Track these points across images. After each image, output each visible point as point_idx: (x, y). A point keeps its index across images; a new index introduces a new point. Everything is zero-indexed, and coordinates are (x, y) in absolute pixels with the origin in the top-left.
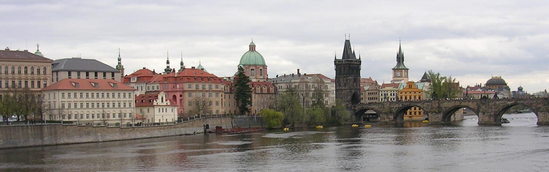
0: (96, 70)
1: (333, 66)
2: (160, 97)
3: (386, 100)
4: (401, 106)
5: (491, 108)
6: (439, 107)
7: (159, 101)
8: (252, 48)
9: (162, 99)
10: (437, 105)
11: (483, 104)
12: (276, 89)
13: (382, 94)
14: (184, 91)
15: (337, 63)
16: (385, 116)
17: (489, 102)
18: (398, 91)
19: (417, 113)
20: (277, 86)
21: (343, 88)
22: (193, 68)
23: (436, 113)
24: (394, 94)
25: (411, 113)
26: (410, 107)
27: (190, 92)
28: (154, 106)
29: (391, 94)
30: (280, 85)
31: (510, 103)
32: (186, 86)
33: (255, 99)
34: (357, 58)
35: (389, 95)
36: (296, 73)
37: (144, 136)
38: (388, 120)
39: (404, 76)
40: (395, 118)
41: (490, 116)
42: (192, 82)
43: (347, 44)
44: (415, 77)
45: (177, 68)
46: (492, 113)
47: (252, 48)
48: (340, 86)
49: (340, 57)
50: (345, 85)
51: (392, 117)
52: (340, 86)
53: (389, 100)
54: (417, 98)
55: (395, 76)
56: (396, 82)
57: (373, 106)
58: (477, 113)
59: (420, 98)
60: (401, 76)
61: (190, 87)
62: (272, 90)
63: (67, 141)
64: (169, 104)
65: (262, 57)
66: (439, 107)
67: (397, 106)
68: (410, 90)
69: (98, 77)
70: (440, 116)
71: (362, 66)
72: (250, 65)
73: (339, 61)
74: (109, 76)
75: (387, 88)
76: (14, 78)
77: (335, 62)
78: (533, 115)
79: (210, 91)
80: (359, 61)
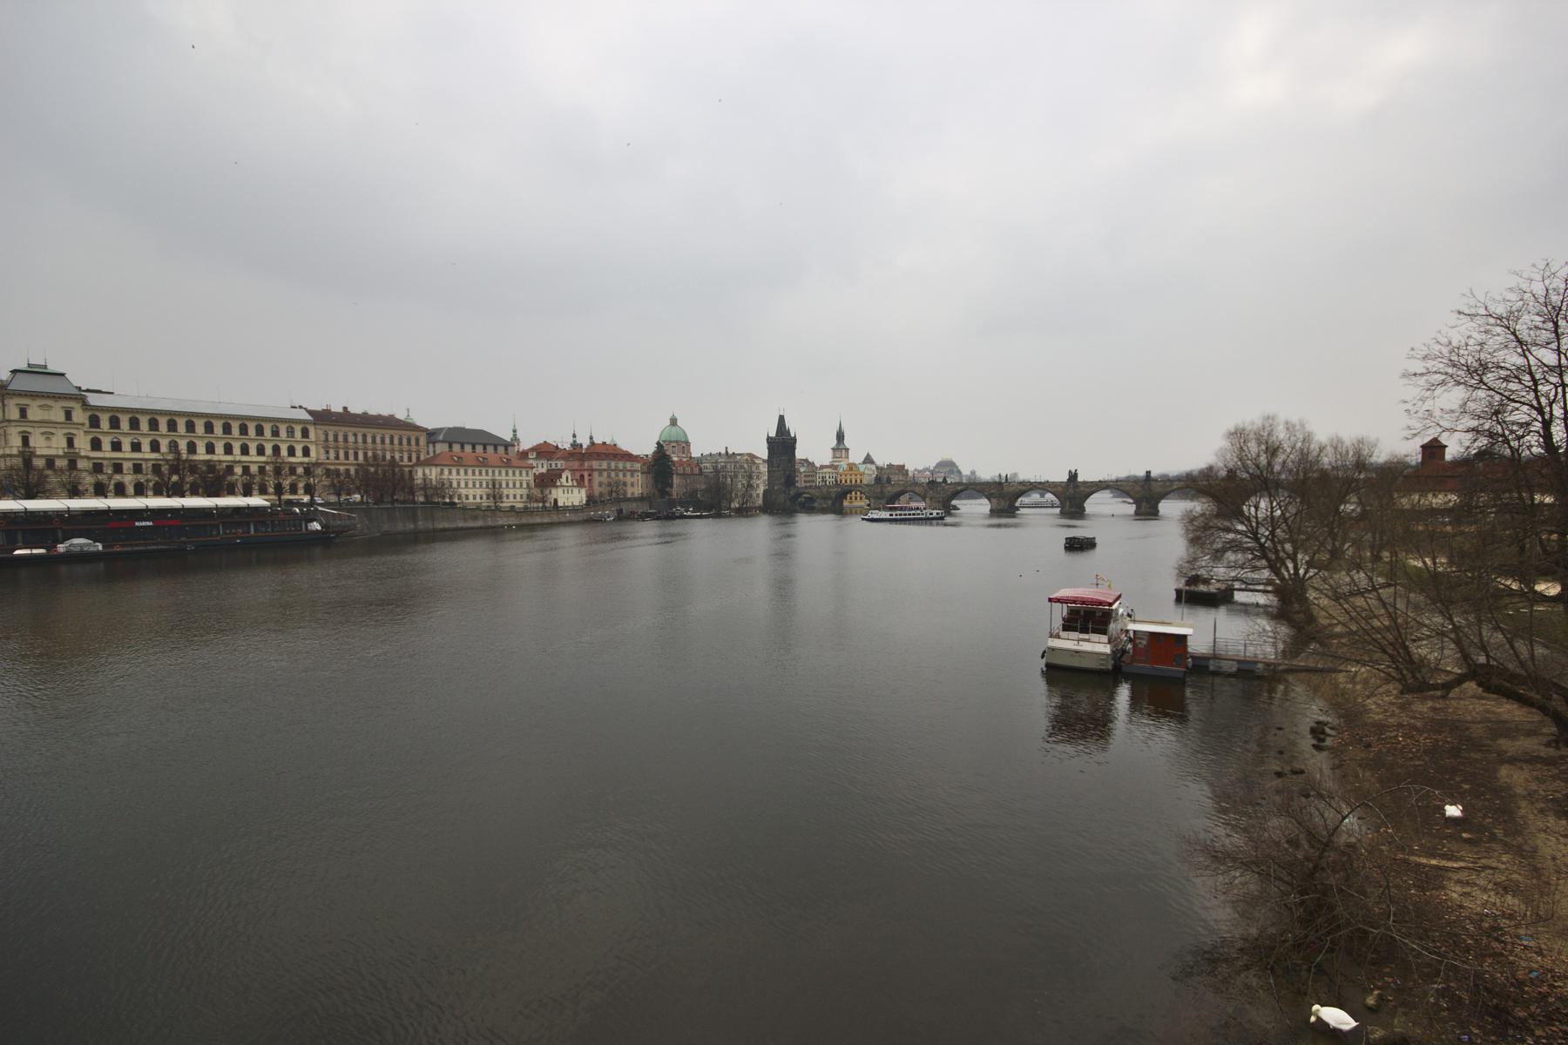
0: (474, 442)
1: (765, 445)
2: (564, 476)
4: (840, 490)
5: (940, 493)
6: (882, 492)
7: (563, 480)
8: (674, 422)
9: (567, 478)
10: (879, 490)
11: (931, 489)
12: (700, 469)
14: (593, 470)
15: (769, 440)
16: (822, 501)
17: (937, 487)
19: (858, 498)
20: (702, 466)
21: (777, 469)
22: (604, 443)
23: (879, 498)
25: (851, 498)
26: (850, 492)
27: (601, 471)
28: (557, 487)
31: (959, 488)
32: (595, 464)
33: (676, 480)
34: (793, 435)
36: (723, 452)
37: (546, 520)
38: (825, 506)
39: (843, 456)
40: (833, 504)
42: (603, 460)
43: (782, 419)
44: (856, 457)
45: (586, 443)
46: (941, 499)
47: (674, 422)
48: (773, 466)
49: (773, 434)
50: (779, 467)
51: (830, 502)
52: (773, 466)
53: (828, 483)
54: (858, 481)
55: (834, 457)
56: (835, 464)
57: (810, 490)
59: (861, 481)
60: (841, 457)
61: (600, 466)
62: (696, 470)
63: (446, 525)
64: (575, 484)
65: (684, 432)
66: (882, 492)
67: (836, 490)
68: (850, 472)
69: (477, 451)
71: (798, 445)
72: (671, 442)
73: (771, 438)
74: (501, 450)
75: (825, 470)
76: (347, 448)
77: (768, 440)
78: (985, 501)
79: (624, 470)
80: (794, 440)
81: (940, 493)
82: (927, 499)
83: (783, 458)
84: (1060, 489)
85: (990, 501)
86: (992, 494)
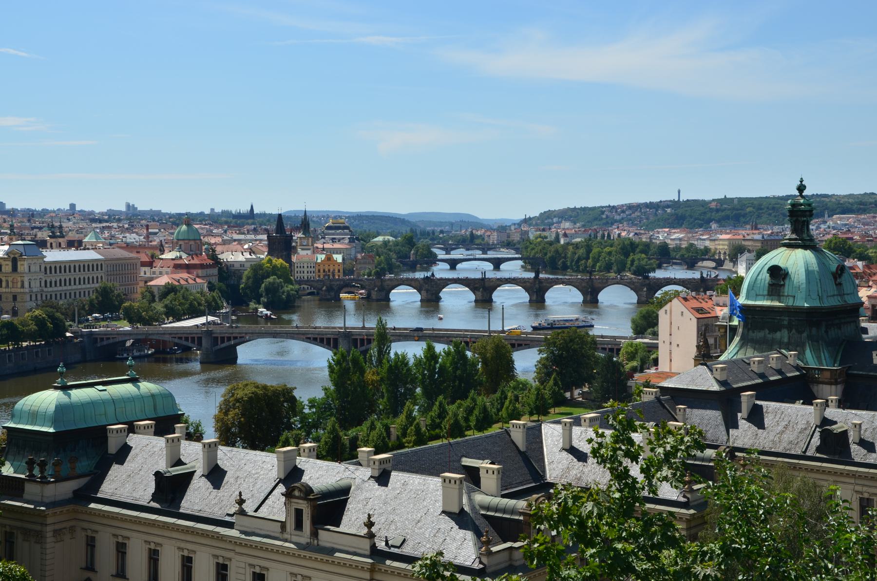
3: (327, 277)
4: (342, 283)
5: (433, 287)
6: (382, 285)
10: (379, 284)
11: (426, 284)
13: (297, 267)
17: (431, 282)
18: (316, 263)
24: (311, 267)
29: (308, 267)
30: (232, 263)
35: (306, 267)
38: (329, 297)
41: (432, 294)
51: (333, 294)
58: (419, 291)
67: (338, 283)
68: (329, 262)
70: (383, 293)
81: (433, 287)
82: (423, 292)
83: (285, 253)
84: (528, 284)
85: (474, 293)
86: (477, 287)
